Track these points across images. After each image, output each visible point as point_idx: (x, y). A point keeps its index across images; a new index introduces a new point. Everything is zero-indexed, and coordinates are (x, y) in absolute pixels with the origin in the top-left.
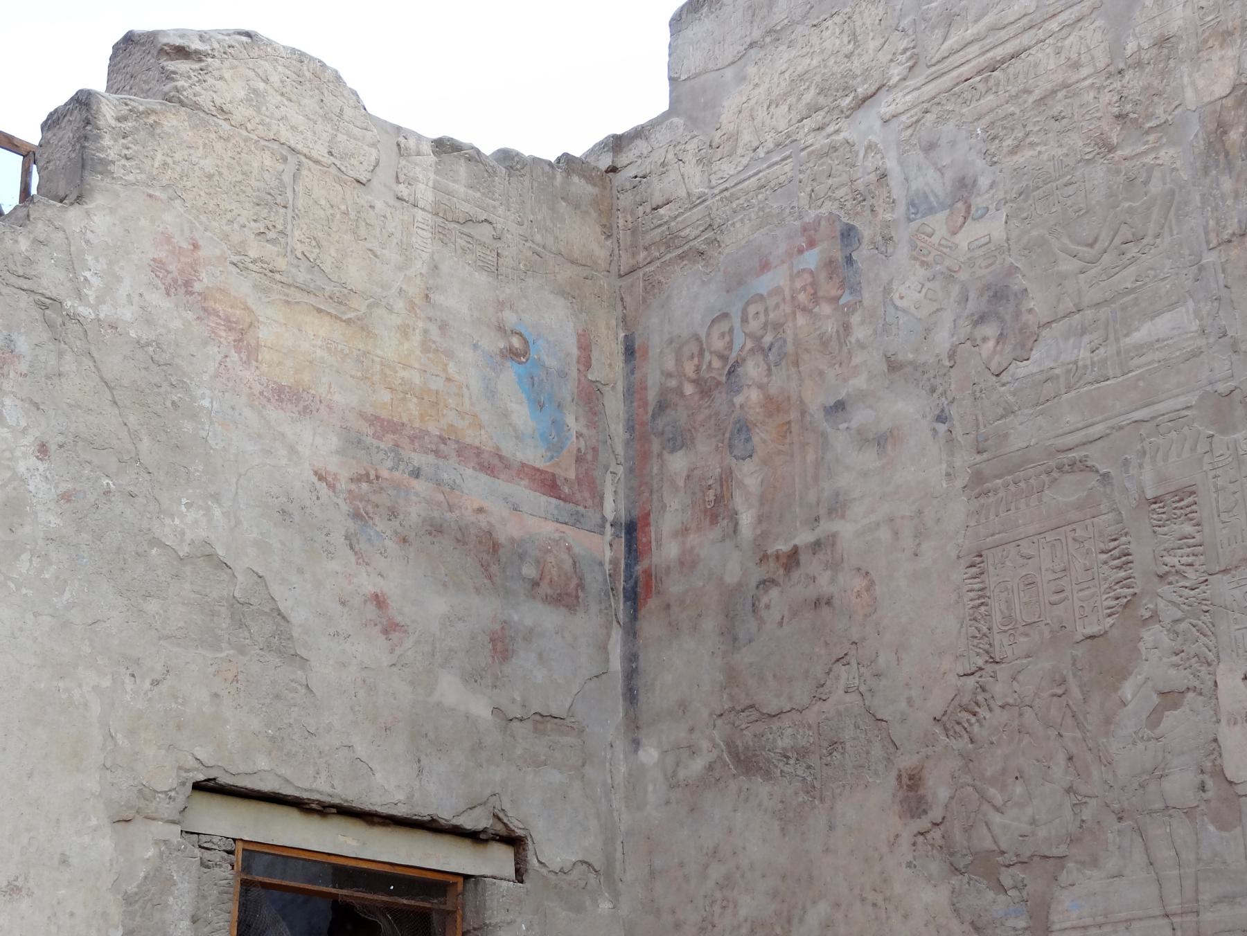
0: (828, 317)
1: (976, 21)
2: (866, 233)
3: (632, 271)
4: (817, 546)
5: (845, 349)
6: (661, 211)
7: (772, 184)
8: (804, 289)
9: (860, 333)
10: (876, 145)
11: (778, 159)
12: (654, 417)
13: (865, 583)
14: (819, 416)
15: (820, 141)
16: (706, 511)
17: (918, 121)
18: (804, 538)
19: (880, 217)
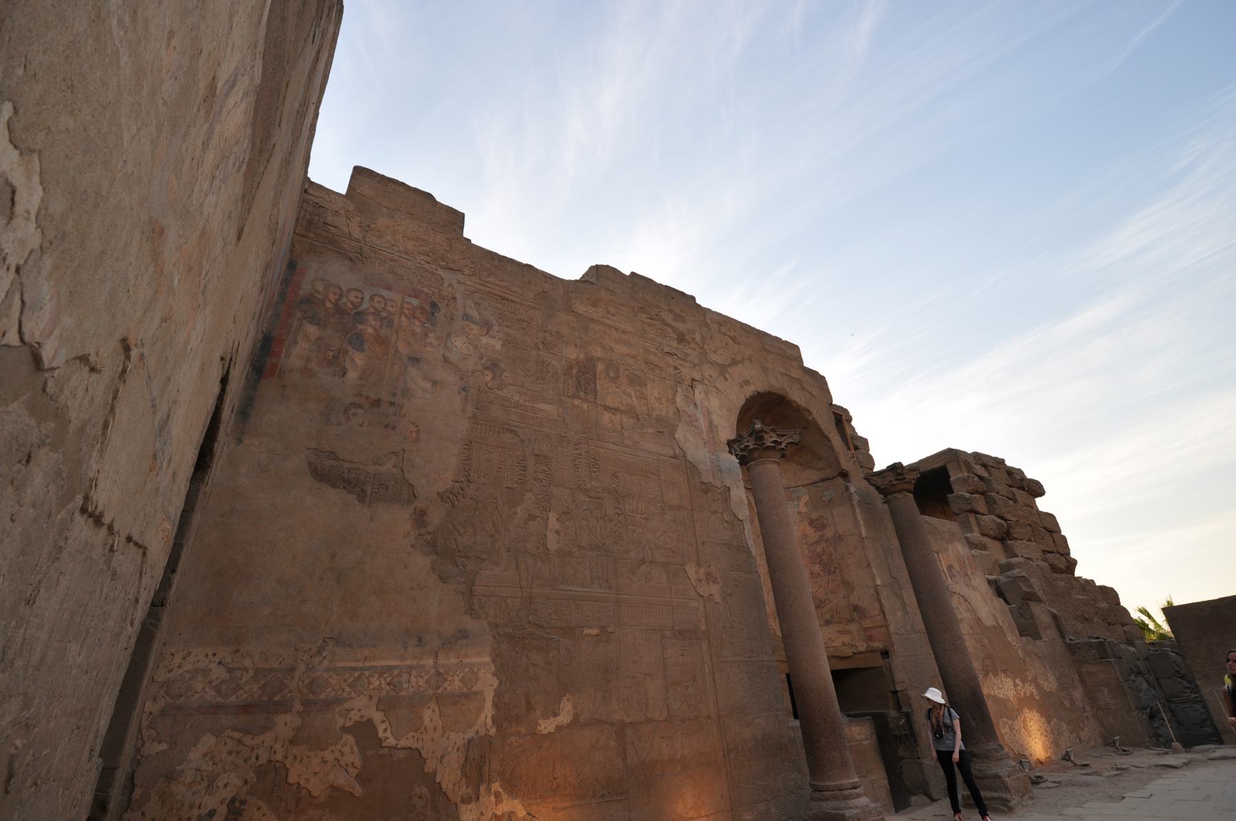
3: (303, 236)
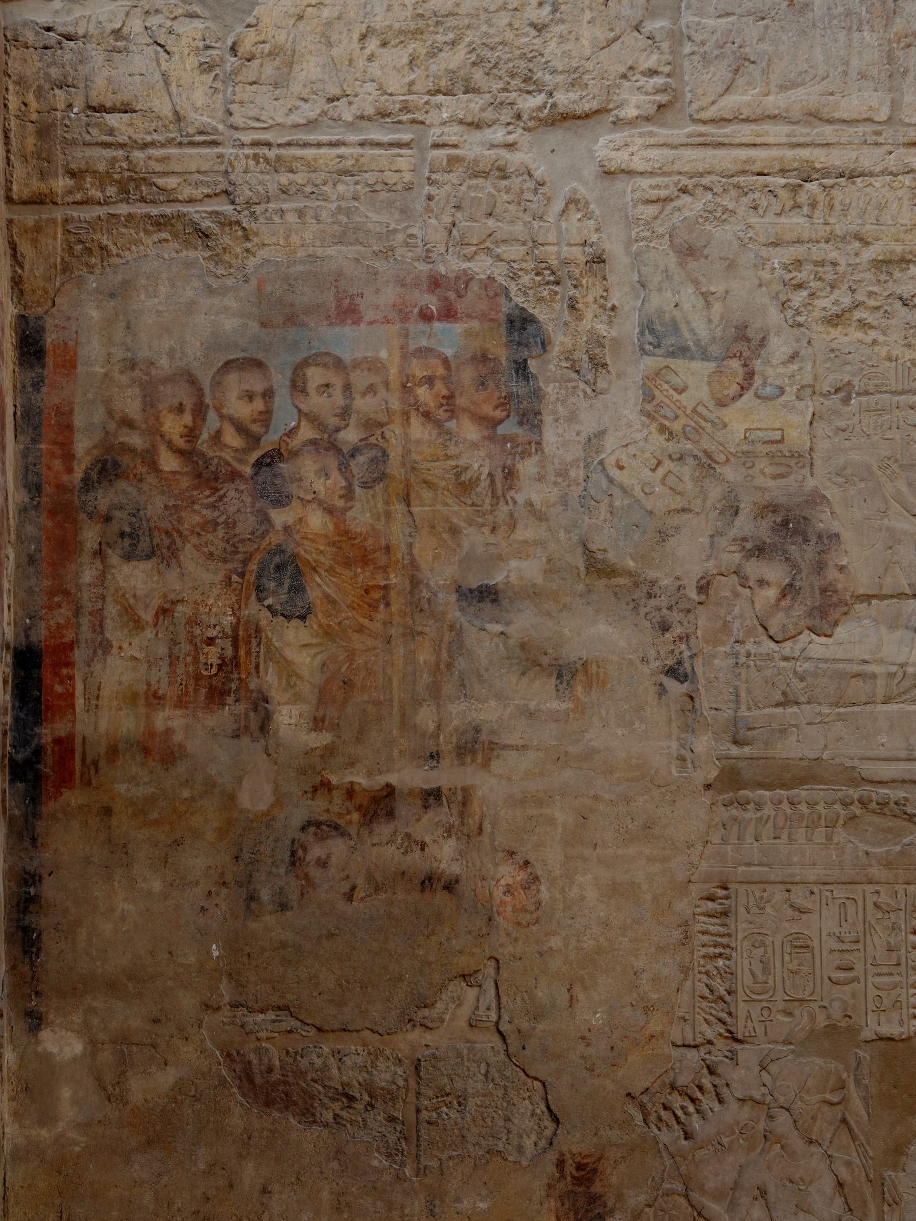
0: (475, 446)
1: (783, 88)
2: (560, 340)
3: (39, 200)
4: (432, 797)
5: (504, 509)
6: (112, 120)
7: (370, 178)
8: (430, 381)
9: (530, 492)
10: (587, 203)
11: (386, 138)
12: (87, 483)
13: (522, 876)
14: (447, 600)
15: (474, 147)
16: (198, 677)
17: (667, 200)
18: (409, 777)
19: (587, 323)
